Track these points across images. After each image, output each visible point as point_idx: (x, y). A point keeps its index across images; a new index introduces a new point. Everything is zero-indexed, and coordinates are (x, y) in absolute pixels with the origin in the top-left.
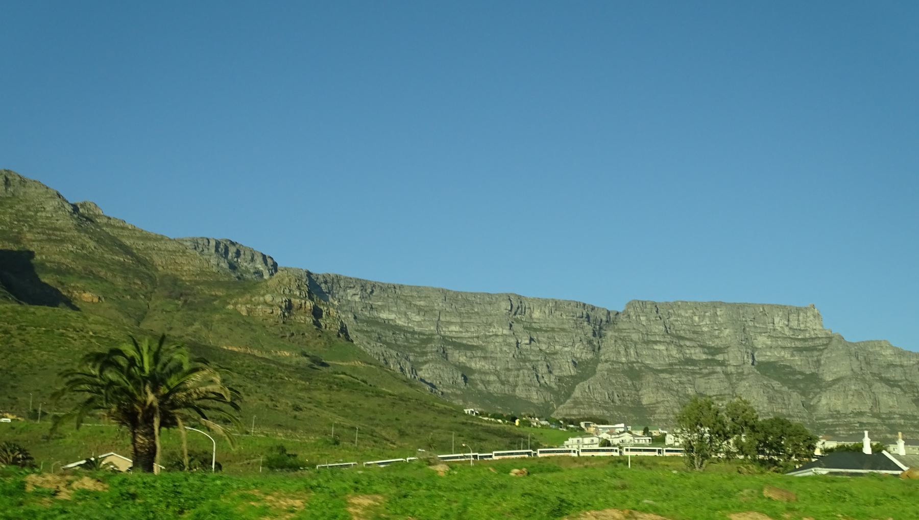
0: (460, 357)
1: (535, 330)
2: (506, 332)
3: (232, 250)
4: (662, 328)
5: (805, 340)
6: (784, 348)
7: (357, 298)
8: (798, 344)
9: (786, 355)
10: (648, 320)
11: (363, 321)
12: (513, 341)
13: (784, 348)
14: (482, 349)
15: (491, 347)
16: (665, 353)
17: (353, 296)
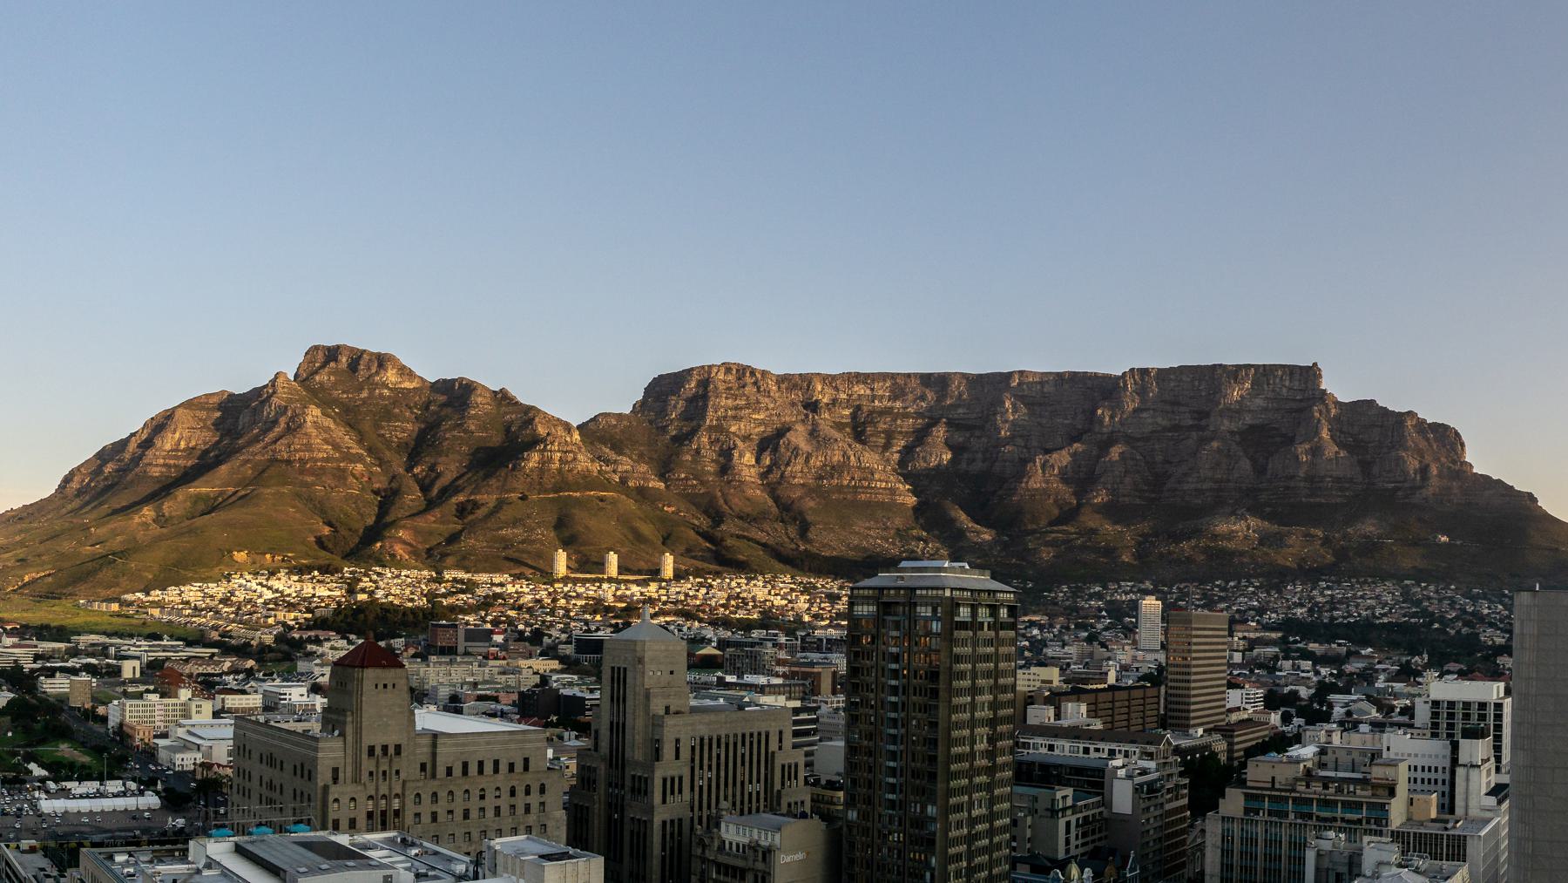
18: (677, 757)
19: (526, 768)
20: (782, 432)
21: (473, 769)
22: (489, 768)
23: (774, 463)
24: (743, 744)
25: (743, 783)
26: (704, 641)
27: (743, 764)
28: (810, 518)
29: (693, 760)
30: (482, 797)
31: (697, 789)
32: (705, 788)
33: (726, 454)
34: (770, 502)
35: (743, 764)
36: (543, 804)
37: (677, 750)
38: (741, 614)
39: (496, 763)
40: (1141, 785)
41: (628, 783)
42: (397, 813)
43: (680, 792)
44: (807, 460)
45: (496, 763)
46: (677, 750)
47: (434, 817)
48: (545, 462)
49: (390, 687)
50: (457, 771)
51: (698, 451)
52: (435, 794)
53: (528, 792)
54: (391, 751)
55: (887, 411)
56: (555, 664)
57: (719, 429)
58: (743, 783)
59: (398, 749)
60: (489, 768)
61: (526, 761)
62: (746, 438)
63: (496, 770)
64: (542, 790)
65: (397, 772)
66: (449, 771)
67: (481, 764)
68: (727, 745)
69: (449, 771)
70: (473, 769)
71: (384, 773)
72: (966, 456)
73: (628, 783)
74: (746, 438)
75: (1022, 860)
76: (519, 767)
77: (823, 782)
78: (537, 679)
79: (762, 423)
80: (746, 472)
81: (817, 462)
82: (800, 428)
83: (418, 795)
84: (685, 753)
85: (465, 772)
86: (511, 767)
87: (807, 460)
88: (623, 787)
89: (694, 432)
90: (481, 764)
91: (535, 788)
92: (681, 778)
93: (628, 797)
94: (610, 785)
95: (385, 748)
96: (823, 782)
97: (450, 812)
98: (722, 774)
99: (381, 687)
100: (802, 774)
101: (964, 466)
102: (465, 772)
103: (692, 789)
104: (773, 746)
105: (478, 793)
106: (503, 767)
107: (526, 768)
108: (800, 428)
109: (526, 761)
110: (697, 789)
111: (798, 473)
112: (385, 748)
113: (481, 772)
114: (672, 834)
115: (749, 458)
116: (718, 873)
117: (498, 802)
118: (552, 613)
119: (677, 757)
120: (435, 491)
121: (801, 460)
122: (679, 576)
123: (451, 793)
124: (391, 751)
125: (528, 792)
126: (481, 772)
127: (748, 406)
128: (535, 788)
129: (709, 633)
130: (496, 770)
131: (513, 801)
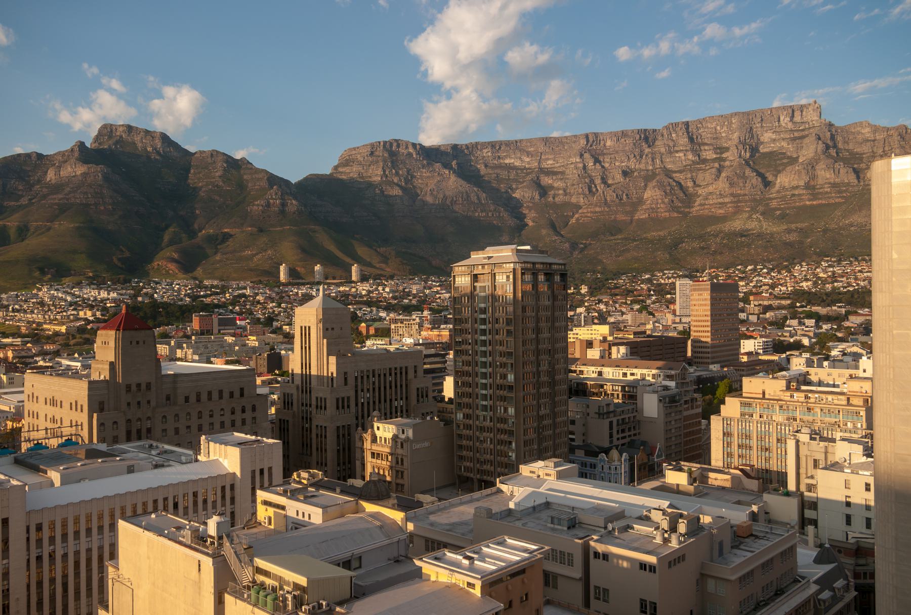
0: (546, 181)
1: (599, 155)
2: (578, 160)
3: (391, 144)
4: (686, 140)
5: (803, 130)
6: (783, 139)
7: (489, 154)
8: (796, 134)
9: (784, 144)
10: (677, 136)
11: (492, 168)
12: (581, 165)
13: (783, 139)
14: (563, 173)
15: (568, 171)
16: (683, 158)
17: (487, 153)
18: (346, 384)
19: (242, 395)
21: (204, 397)
22: (215, 396)
24: (390, 374)
25: (391, 400)
26: (381, 319)
27: (391, 387)
29: (356, 386)
30: (211, 416)
31: (360, 405)
32: (366, 404)
35: (391, 387)
36: (254, 418)
37: (346, 379)
38: (406, 301)
39: (221, 392)
40: (664, 397)
41: (314, 403)
42: (149, 430)
43: (348, 407)
45: (221, 392)
46: (346, 379)
47: (177, 431)
49: (141, 343)
50: (193, 399)
52: (177, 415)
53: (243, 411)
54: (143, 387)
55: (500, 167)
56: (280, 338)
58: (391, 400)
59: (148, 386)
60: (215, 396)
61: (242, 390)
63: (221, 397)
64: (254, 409)
65: (149, 402)
66: (187, 399)
67: (210, 393)
68: (379, 375)
69: (187, 399)
70: (204, 397)
71: (139, 403)
72: (552, 192)
73: (314, 403)
75: (579, 447)
76: (237, 394)
77: (446, 400)
78: (268, 347)
83: (164, 417)
84: (351, 381)
85: (198, 400)
86: (232, 395)
88: (310, 406)
90: (210, 393)
91: (248, 408)
92: (348, 398)
93: (314, 412)
94: (302, 404)
95: (139, 385)
96: (446, 400)
97: (188, 427)
98: (377, 394)
99: (134, 343)
100: (431, 395)
101: (551, 199)
102: (198, 400)
103: (357, 405)
104: (411, 374)
105: (208, 413)
106: (226, 395)
107: (242, 395)
109: (242, 390)
110: (360, 405)
112: (139, 385)
113: (210, 399)
114: (344, 435)
116: (373, 457)
117: (223, 419)
118: (279, 306)
119: (346, 384)
122: (364, 279)
123: (189, 414)
124: (143, 387)
125: (243, 411)
126: (210, 399)
128: (248, 408)
129: (383, 314)
130: (221, 397)
131: (233, 417)
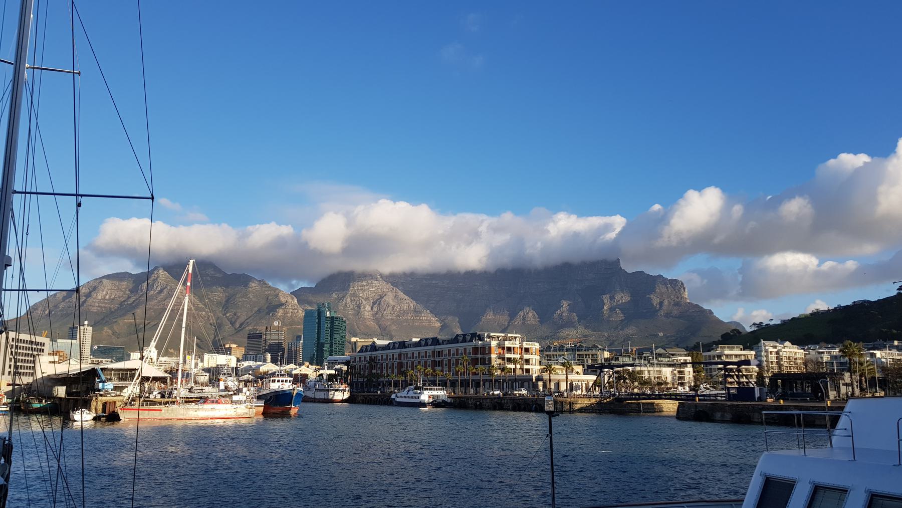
20: (381, 298)
23: (379, 310)
28: (393, 334)
33: (359, 307)
34: (377, 327)
44: (393, 308)
48: (285, 313)
51: (346, 305)
57: (355, 295)
62: (367, 299)
74: (367, 299)
79: (373, 292)
80: (366, 314)
81: (397, 309)
82: (390, 294)
87: (393, 308)
89: (344, 297)
108: (390, 294)
111: (388, 314)
115: (368, 308)
120: (237, 325)
121: (390, 308)
127: (367, 285)
